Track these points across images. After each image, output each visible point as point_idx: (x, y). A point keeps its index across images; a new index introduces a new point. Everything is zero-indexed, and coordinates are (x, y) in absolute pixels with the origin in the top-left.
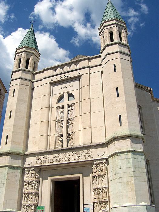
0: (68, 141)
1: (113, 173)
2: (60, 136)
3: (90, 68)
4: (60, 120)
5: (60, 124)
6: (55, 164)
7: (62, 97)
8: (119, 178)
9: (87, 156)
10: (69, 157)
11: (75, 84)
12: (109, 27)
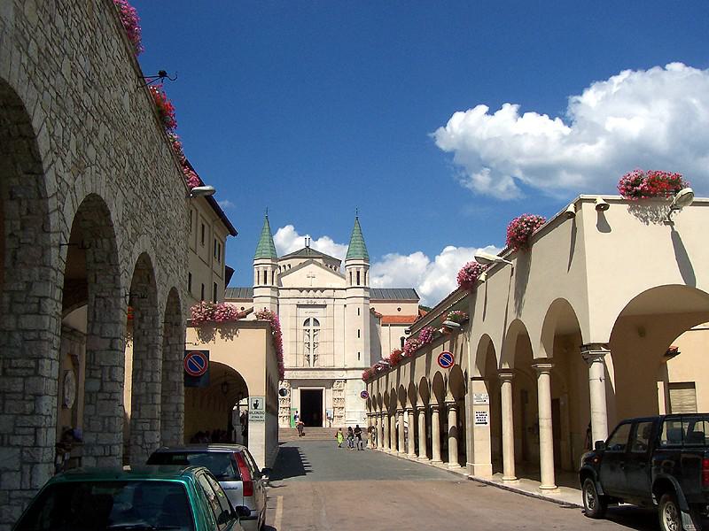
11: (321, 310)
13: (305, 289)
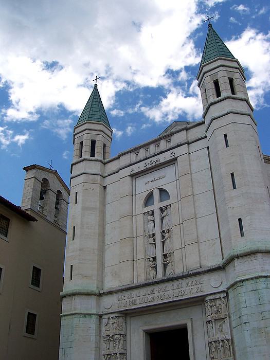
0: (165, 266)
1: (236, 315)
2: (152, 259)
3: (189, 143)
4: (151, 234)
5: (151, 240)
6: (147, 306)
7: (150, 196)
8: (245, 323)
9: (194, 291)
10: (167, 293)
11: (169, 171)
12: (212, 72)
13: (140, 147)
